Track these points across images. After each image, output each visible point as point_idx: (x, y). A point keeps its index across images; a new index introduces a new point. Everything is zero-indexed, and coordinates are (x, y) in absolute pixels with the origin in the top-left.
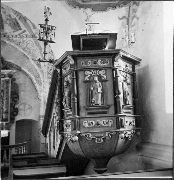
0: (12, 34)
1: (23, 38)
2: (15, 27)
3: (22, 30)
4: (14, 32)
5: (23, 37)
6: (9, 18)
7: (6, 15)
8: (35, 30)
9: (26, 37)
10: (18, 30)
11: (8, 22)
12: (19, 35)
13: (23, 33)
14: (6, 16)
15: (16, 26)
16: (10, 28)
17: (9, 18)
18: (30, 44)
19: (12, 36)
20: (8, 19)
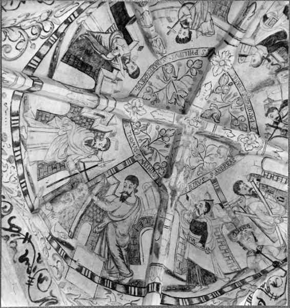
0: (82, 17)
1: (45, 40)
2: (81, 45)
3: (61, 61)
4: (80, 28)
5: (46, 43)
6: (110, 56)
7: (119, 55)
8: (35, 112)
9: (38, 54)
10: (70, 46)
11: (106, 39)
12: (62, 35)
13: (55, 54)
14: (116, 54)
15: (82, 49)
16: (95, 29)
17: (110, 56)
18: (13, 45)
19: (80, 11)
20: (109, 50)
